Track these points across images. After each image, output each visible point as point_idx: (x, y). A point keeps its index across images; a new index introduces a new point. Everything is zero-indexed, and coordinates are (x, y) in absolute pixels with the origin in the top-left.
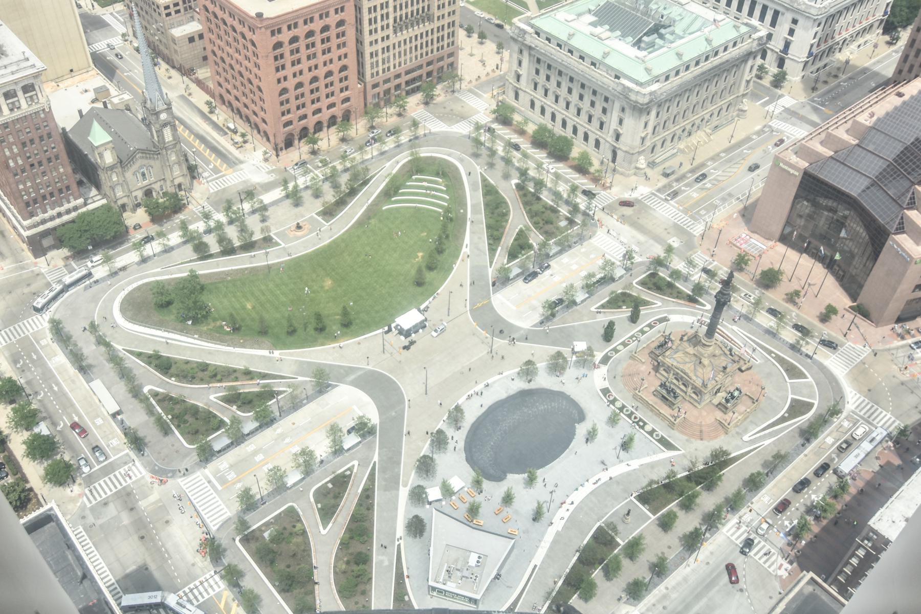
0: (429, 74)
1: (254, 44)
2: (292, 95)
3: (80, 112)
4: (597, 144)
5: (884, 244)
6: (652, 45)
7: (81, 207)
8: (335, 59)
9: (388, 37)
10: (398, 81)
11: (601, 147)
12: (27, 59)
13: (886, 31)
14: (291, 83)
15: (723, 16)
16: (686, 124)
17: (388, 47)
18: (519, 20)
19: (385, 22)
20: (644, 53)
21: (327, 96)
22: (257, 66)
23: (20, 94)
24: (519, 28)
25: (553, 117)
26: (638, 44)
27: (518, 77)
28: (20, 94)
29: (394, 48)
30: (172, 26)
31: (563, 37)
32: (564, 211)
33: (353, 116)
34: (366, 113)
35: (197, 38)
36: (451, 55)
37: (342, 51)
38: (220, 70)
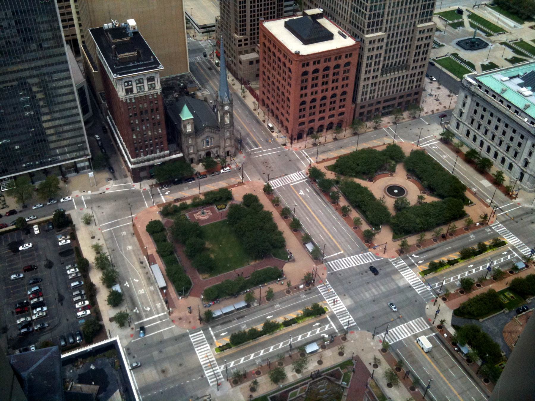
0: (399, 104)
2: (307, 106)
4: (511, 167)
9: (377, 76)
10: (378, 106)
11: (513, 169)
14: (308, 99)
17: (376, 83)
18: (469, 76)
21: (330, 110)
22: (289, 85)
24: (468, 81)
27: (461, 113)
28: (145, 82)
30: (241, 53)
35: (255, 62)
36: (416, 93)
37: (345, 82)
38: (266, 84)
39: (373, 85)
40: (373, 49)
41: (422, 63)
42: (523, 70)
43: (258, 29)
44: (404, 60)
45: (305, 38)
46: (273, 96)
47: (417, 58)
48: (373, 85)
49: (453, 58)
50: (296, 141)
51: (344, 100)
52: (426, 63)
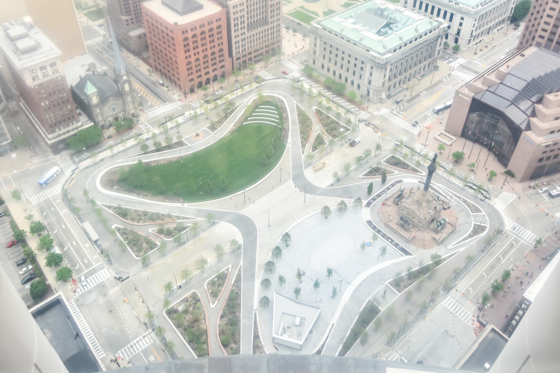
0: (267, 52)
1: (173, 39)
3: (80, 76)
4: (359, 87)
6: (386, 33)
8: (217, 46)
9: (244, 33)
10: (250, 56)
12: (52, 50)
13: (512, 22)
14: (193, 59)
16: (407, 74)
17: (244, 39)
20: (382, 37)
21: (212, 65)
22: (175, 50)
23: (48, 68)
25: (334, 73)
26: (379, 33)
28: (48, 68)
30: (130, 31)
31: (338, 30)
32: (341, 123)
33: (226, 74)
34: (233, 73)
37: (220, 41)
38: (155, 53)
40: (237, 12)
42: (352, 11)
43: (140, 9)
45: (180, 10)
46: (163, 61)
48: (243, 41)
49: (301, 10)
50: (189, 95)
51: (222, 55)
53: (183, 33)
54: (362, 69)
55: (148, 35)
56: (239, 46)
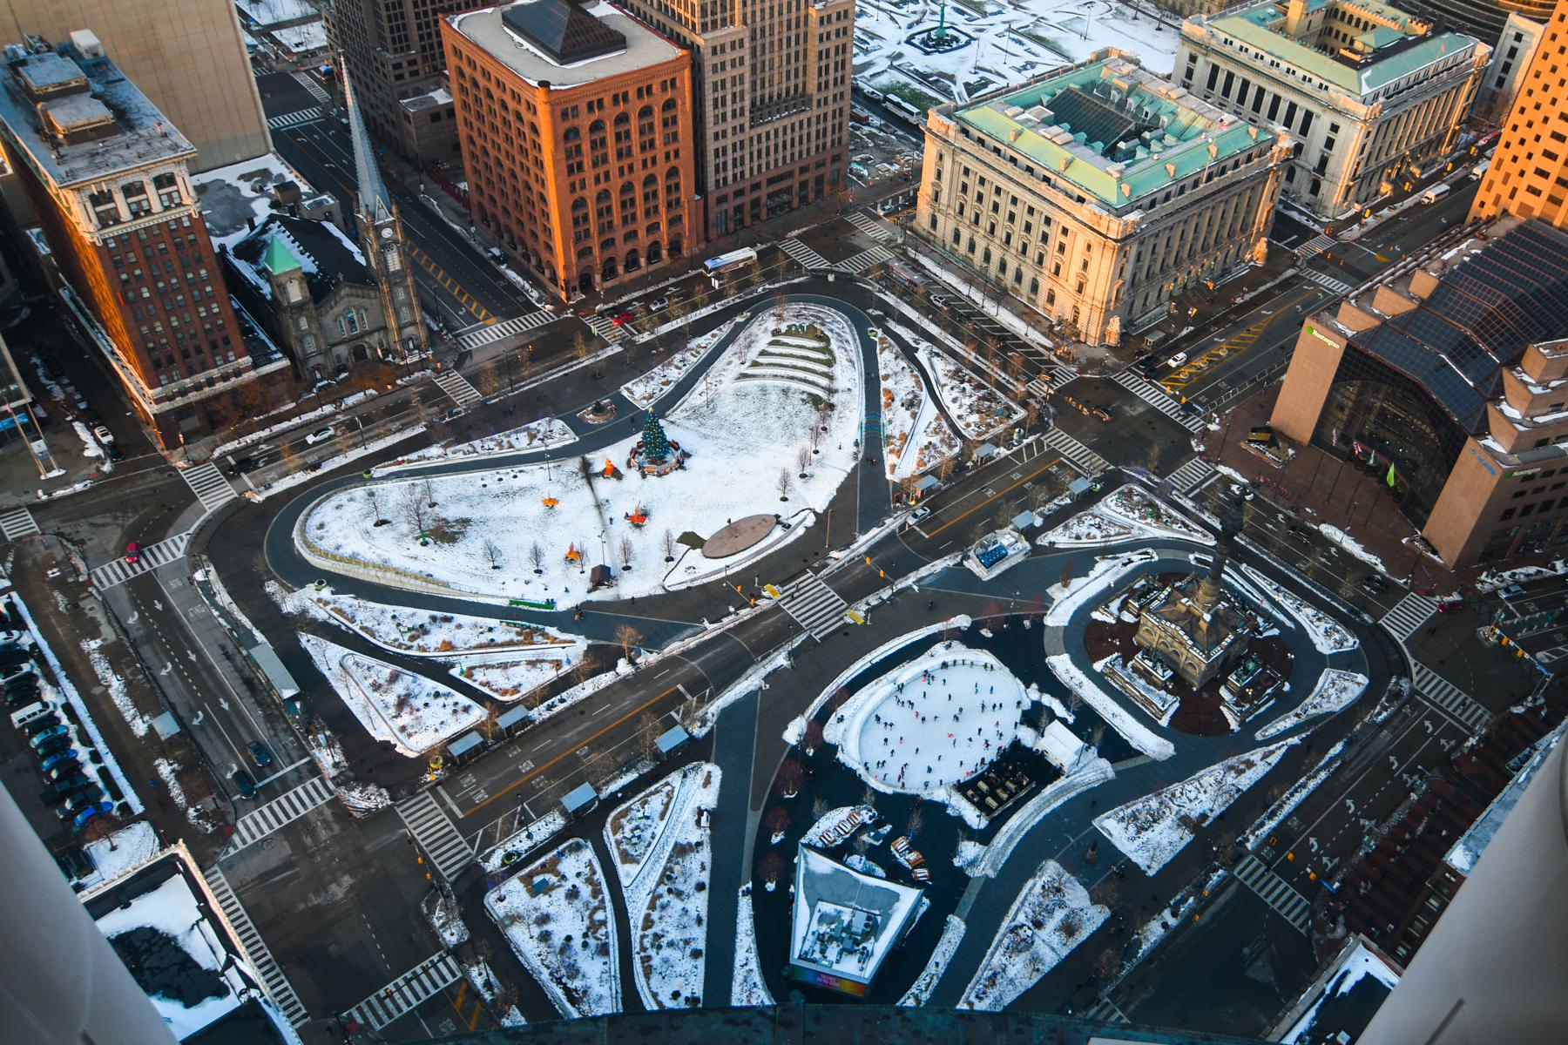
0: (803, 185)
5: (1460, 450)
6: (1131, 154)
7: (247, 369)
9: (742, 126)
10: (756, 194)
14: (591, 193)
15: (1234, 118)
17: (742, 142)
19: (738, 106)
20: (1121, 166)
22: (540, 164)
26: (1111, 153)
29: (751, 145)
36: (836, 159)
37: (672, 148)
39: (742, 147)
41: (837, 91)
44: (796, 86)
47: (823, 79)
52: (847, 89)
53: (565, 114)
54: (1062, 248)
55: (459, 113)
56: (725, 164)
